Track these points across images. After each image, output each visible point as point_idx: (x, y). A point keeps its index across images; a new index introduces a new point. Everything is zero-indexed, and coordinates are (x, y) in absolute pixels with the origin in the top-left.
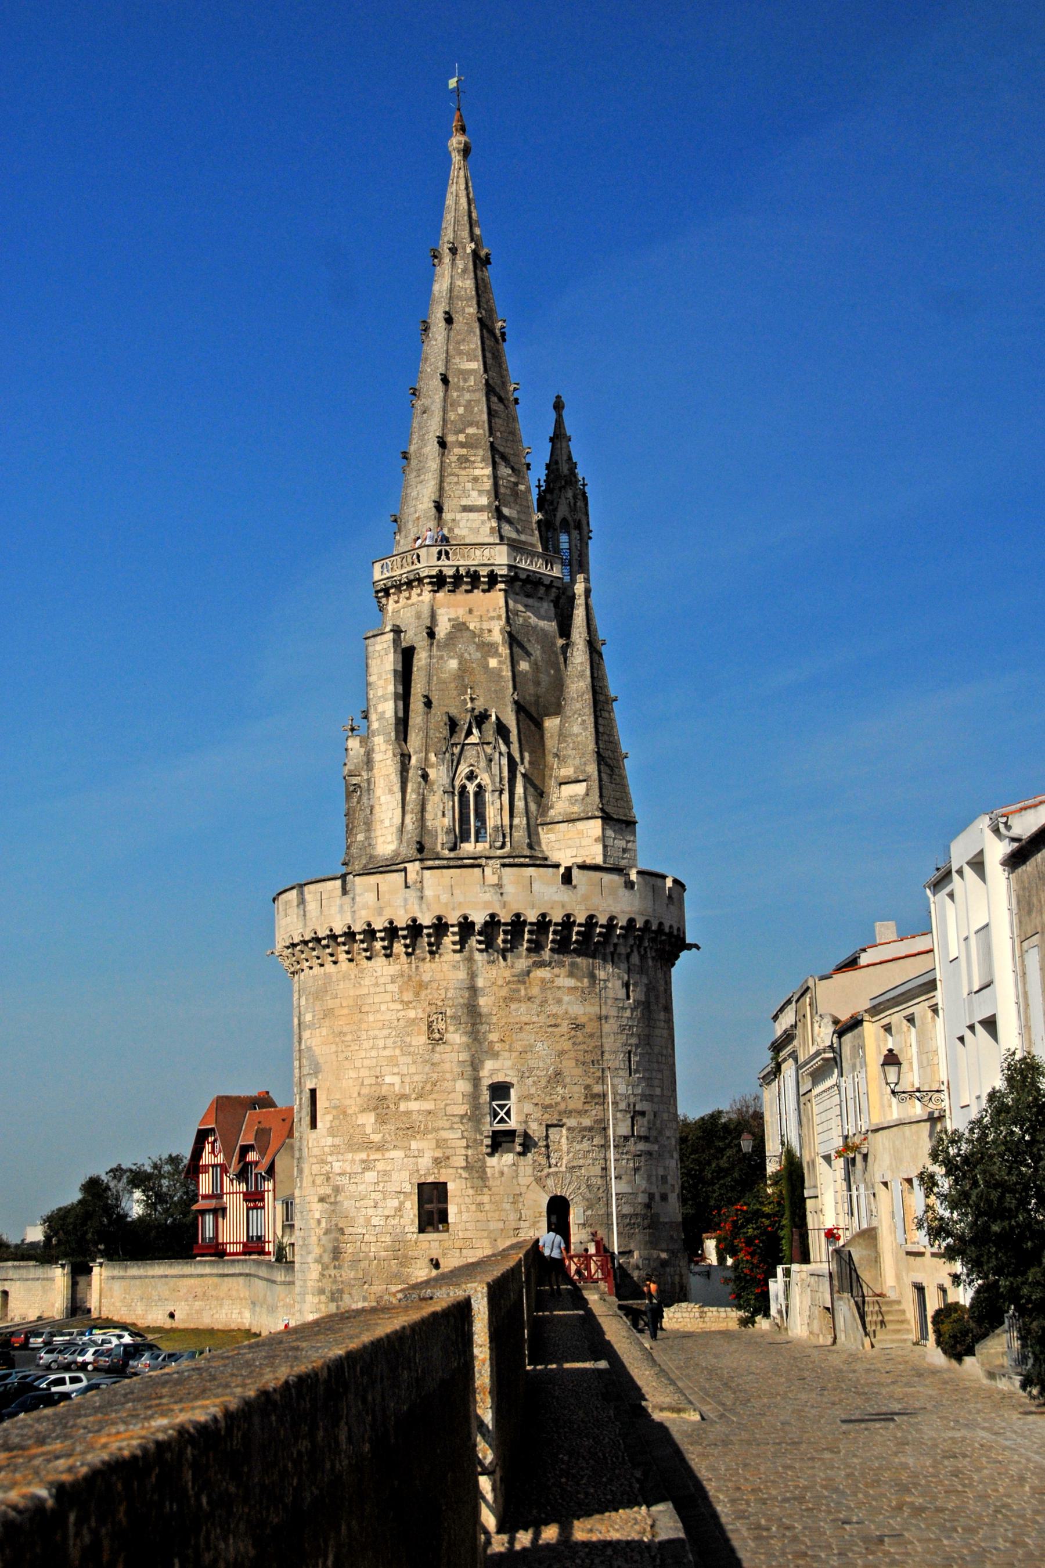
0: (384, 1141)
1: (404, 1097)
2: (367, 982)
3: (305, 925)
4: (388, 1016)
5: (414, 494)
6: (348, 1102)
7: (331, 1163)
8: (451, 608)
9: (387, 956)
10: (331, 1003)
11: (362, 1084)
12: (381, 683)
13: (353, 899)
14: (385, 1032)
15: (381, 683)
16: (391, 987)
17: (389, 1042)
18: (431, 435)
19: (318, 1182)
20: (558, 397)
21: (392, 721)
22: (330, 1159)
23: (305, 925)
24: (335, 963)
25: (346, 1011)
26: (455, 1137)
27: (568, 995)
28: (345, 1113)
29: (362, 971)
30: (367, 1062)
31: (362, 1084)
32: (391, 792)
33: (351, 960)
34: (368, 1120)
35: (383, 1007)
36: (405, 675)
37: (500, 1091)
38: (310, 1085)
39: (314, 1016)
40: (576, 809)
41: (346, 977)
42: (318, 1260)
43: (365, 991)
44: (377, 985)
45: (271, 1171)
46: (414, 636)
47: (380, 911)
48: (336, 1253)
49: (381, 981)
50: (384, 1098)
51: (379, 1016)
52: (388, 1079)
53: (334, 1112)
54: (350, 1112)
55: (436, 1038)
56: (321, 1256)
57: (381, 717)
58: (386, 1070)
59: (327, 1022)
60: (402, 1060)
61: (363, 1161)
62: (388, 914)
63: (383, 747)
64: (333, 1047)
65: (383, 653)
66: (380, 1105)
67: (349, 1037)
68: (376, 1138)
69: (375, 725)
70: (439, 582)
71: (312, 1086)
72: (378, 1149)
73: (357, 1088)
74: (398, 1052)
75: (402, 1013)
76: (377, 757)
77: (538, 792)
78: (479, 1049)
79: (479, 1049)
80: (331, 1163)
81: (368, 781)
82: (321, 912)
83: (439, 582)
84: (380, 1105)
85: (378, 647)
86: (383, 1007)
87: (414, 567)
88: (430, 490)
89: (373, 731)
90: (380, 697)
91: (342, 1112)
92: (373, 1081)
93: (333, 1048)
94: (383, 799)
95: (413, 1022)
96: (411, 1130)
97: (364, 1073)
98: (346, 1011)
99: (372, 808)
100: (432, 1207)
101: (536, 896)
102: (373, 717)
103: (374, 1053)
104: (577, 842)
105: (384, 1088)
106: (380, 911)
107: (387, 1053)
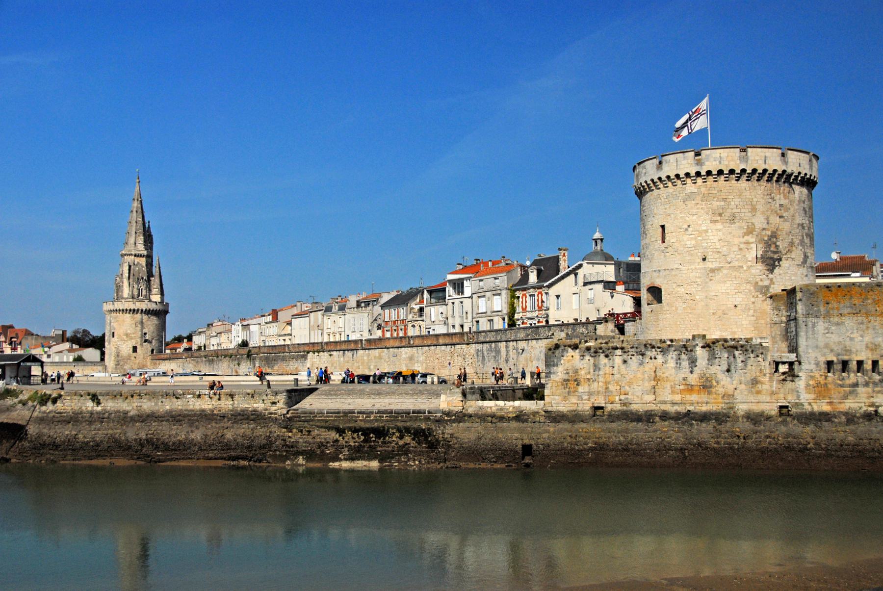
8: (137, 260)
26: (139, 340)
27: (154, 320)
36: (129, 270)
37: (145, 334)
45: (20, 344)
46: (132, 264)
55: (136, 326)
66: (127, 335)
70: (135, 256)
77: (150, 290)
78: (143, 328)
79: (143, 328)
83: (135, 256)
84: (127, 335)
91: (120, 336)
96: (132, 339)
100: (135, 349)
101: (153, 306)
104: (156, 298)
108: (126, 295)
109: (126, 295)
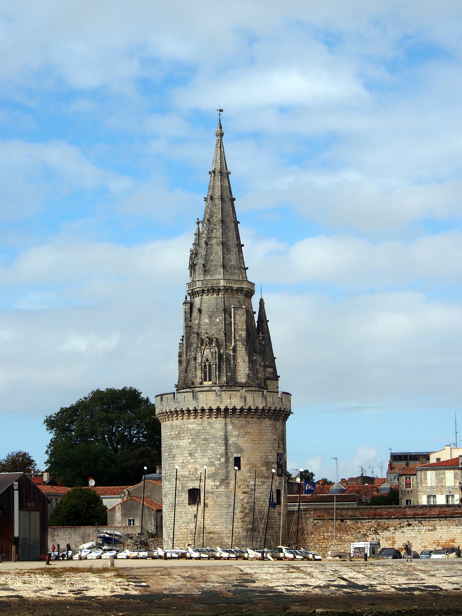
0: (268, 476)
1: (273, 463)
2: (264, 425)
3: (245, 404)
4: (269, 437)
5: (227, 257)
6: (257, 463)
7: (249, 482)
9: (269, 418)
10: (249, 430)
11: (262, 457)
12: (240, 324)
13: (266, 399)
14: (269, 442)
15: (240, 324)
16: (270, 428)
17: (270, 445)
18: (231, 238)
19: (242, 487)
20: (198, 219)
21: (245, 338)
22: (248, 480)
23: (245, 404)
24: (252, 418)
25: (256, 434)
28: (256, 466)
29: (261, 422)
30: (263, 451)
31: (262, 457)
32: (244, 362)
33: (258, 418)
34: (264, 469)
35: (268, 434)
38: (235, 455)
39: (239, 434)
40: (271, 376)
41: (256, 423)
42: (242, 512)
43: (262, 428)
44: (266, 427)
47: (273, 404)
48: (253, 510)
49: (267, 426)
50: (268, 463)
51: (267, 437)
52: (270, 457)
53: (251, 465)
54: (258, 466)
56: (244, 510)
57: (240, 336)
58: (269, 454)
59: (247, 436)
60: (273, 451)
61: (262, 482)
62: (276, 405)
63: (241, 346)
64: (250, 445)
65: (241, 314)
67: (257, 442)
68: (266, 475)
69: (238, 338)
71: (239, 456)
72: (267, 478)
73: (260, 459)
74: (272, 449)
75: (272, 437)
76: (238, 349)
80: (249, 482)
81: (234, 356)
82: (254, 401)
85: (239, 312)
86: (268, 434)
87: (241, 286)
88: (234, 258)
89: (237, 340)
90: (239, 329)
92: (265, 457)
93: (250, 445)
94: (240, 363)
95: (275, 440)
97: (263, 454)
98: (256, 434)
99: (236, 365)
102: (237, 335)
103: (265, 448)
105: (269, 459)
106: (273, 404)
107: (269, 448)
108: (242, 377)
109: (242, 377)
